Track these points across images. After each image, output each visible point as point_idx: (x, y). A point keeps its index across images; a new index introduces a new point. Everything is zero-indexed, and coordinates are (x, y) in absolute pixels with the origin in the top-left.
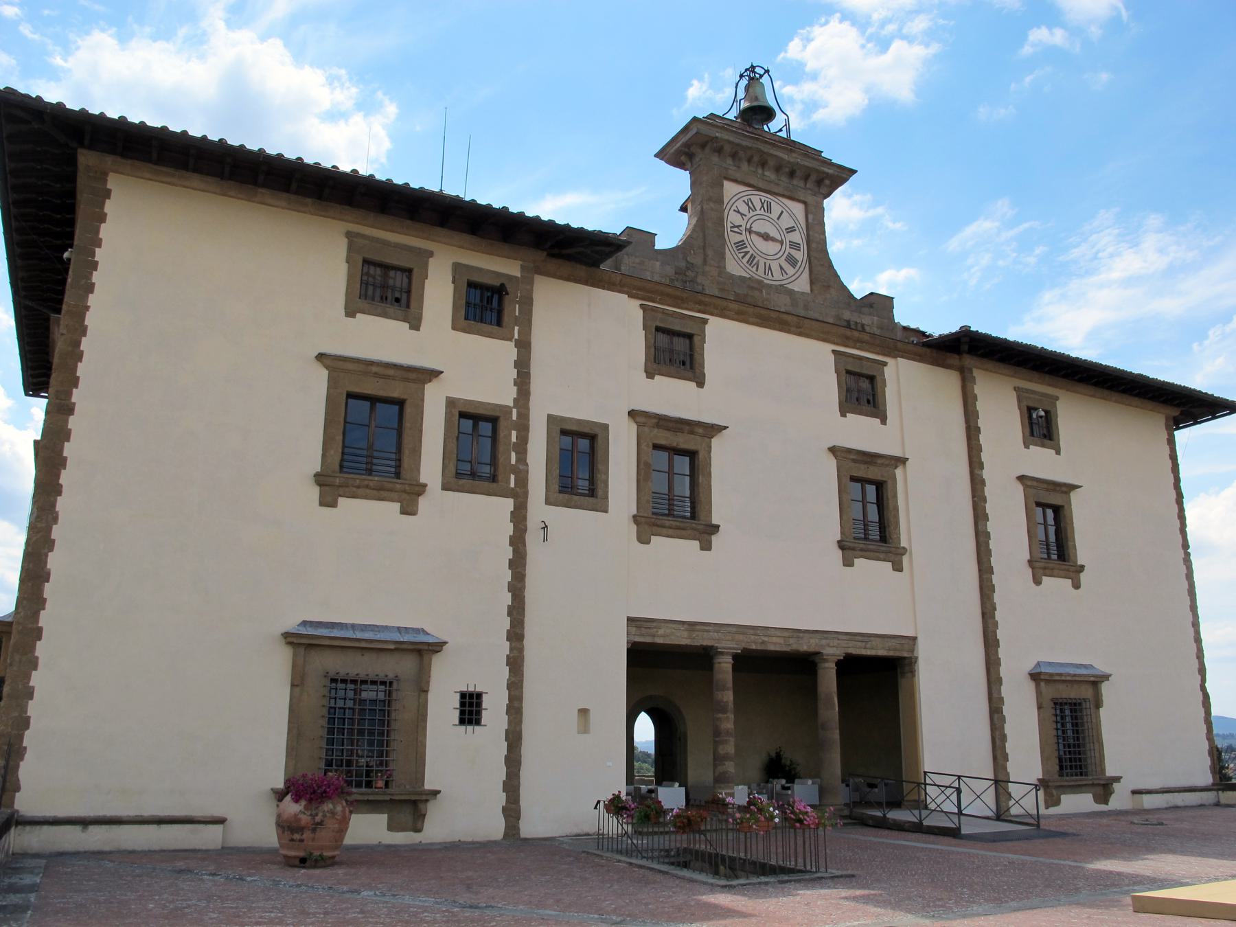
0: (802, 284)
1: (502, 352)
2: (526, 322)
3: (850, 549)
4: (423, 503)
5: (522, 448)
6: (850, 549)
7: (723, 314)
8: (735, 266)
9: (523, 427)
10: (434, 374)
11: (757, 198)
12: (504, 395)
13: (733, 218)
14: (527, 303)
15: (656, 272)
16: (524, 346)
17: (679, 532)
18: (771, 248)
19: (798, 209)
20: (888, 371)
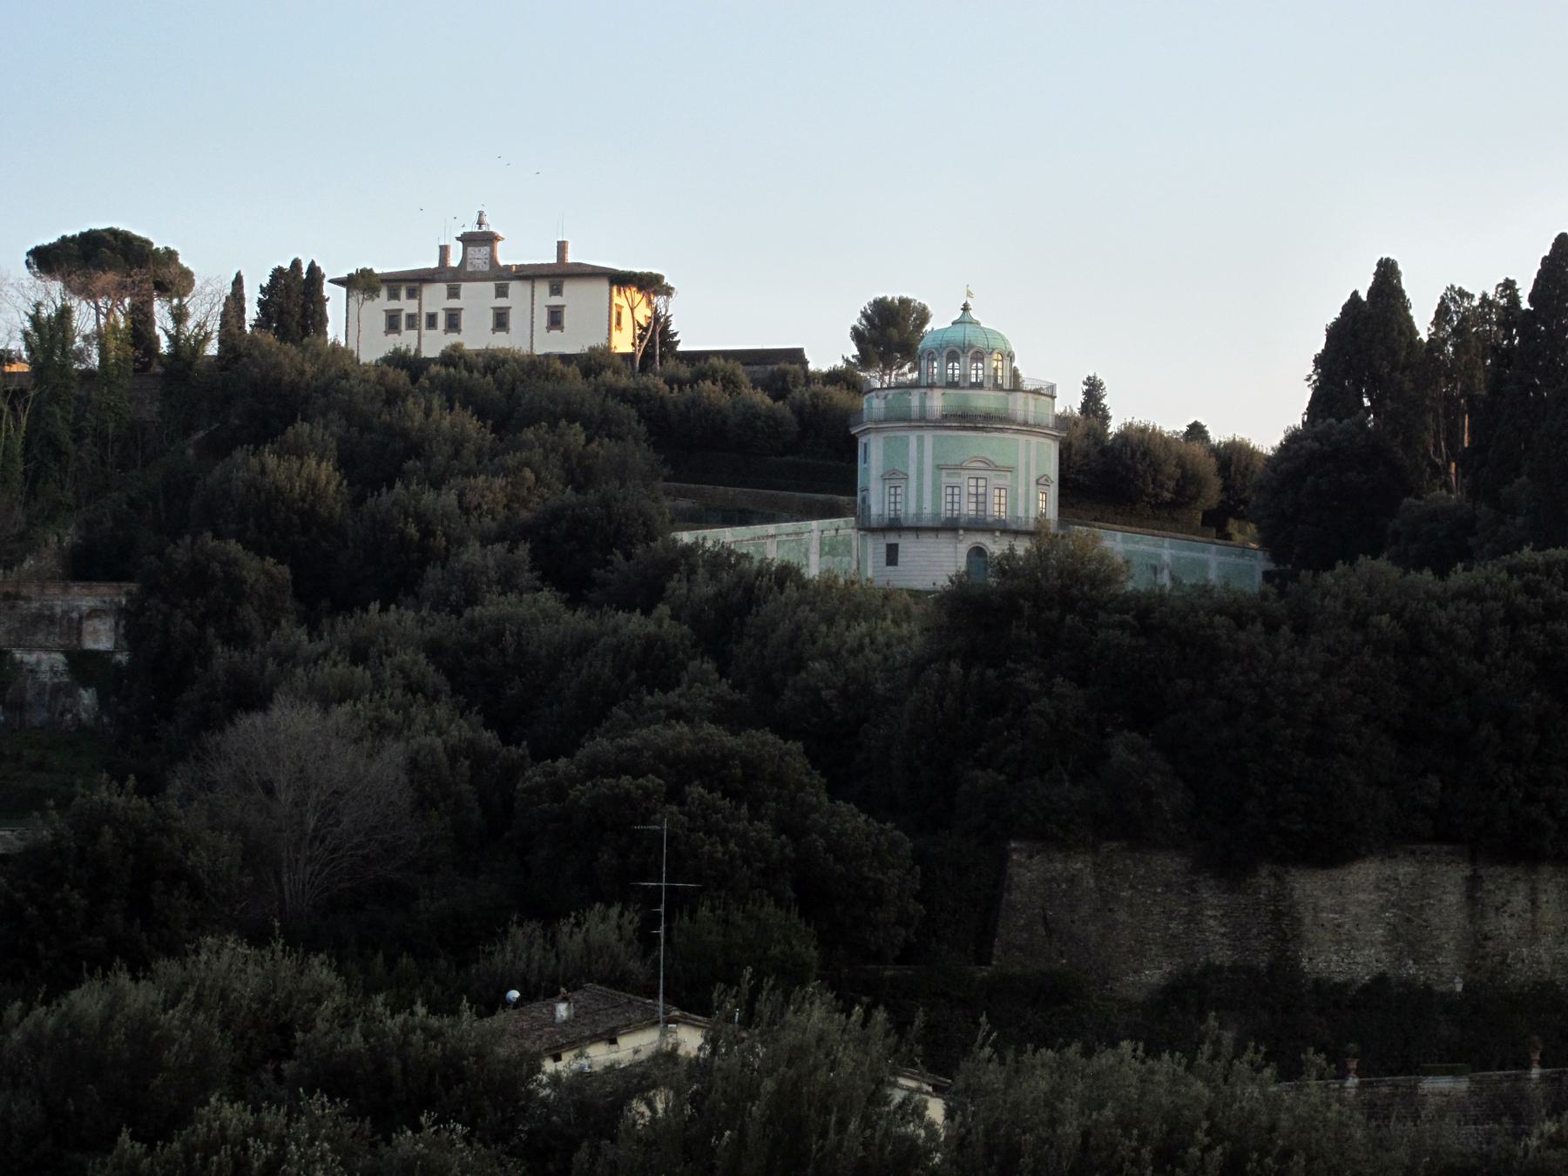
0: (487, 268)
1: (415, 302)
2: (420, 295)
3: (494, 330)
4: (402, 334)
5: (420, 321)
6: (494, 330)
7: (464, 281)
8: (469, 269)
9: (420, 316)
10: (401, 310)
11: (477, 249)
12: (416, 311)
13: (470, 256)
14: (421, 291)
15: (448, 275)
16: (420, 300)
17: (452, 332)
18: (479, 261)
19: (488, 248)
20: (510, 286)
